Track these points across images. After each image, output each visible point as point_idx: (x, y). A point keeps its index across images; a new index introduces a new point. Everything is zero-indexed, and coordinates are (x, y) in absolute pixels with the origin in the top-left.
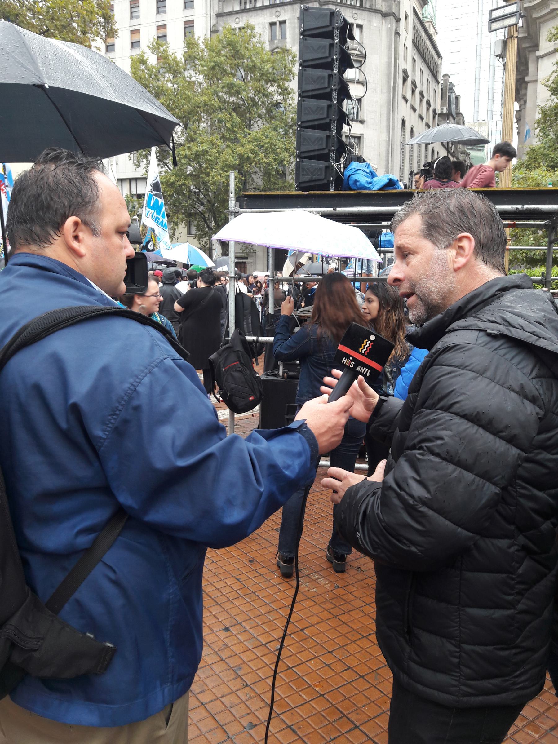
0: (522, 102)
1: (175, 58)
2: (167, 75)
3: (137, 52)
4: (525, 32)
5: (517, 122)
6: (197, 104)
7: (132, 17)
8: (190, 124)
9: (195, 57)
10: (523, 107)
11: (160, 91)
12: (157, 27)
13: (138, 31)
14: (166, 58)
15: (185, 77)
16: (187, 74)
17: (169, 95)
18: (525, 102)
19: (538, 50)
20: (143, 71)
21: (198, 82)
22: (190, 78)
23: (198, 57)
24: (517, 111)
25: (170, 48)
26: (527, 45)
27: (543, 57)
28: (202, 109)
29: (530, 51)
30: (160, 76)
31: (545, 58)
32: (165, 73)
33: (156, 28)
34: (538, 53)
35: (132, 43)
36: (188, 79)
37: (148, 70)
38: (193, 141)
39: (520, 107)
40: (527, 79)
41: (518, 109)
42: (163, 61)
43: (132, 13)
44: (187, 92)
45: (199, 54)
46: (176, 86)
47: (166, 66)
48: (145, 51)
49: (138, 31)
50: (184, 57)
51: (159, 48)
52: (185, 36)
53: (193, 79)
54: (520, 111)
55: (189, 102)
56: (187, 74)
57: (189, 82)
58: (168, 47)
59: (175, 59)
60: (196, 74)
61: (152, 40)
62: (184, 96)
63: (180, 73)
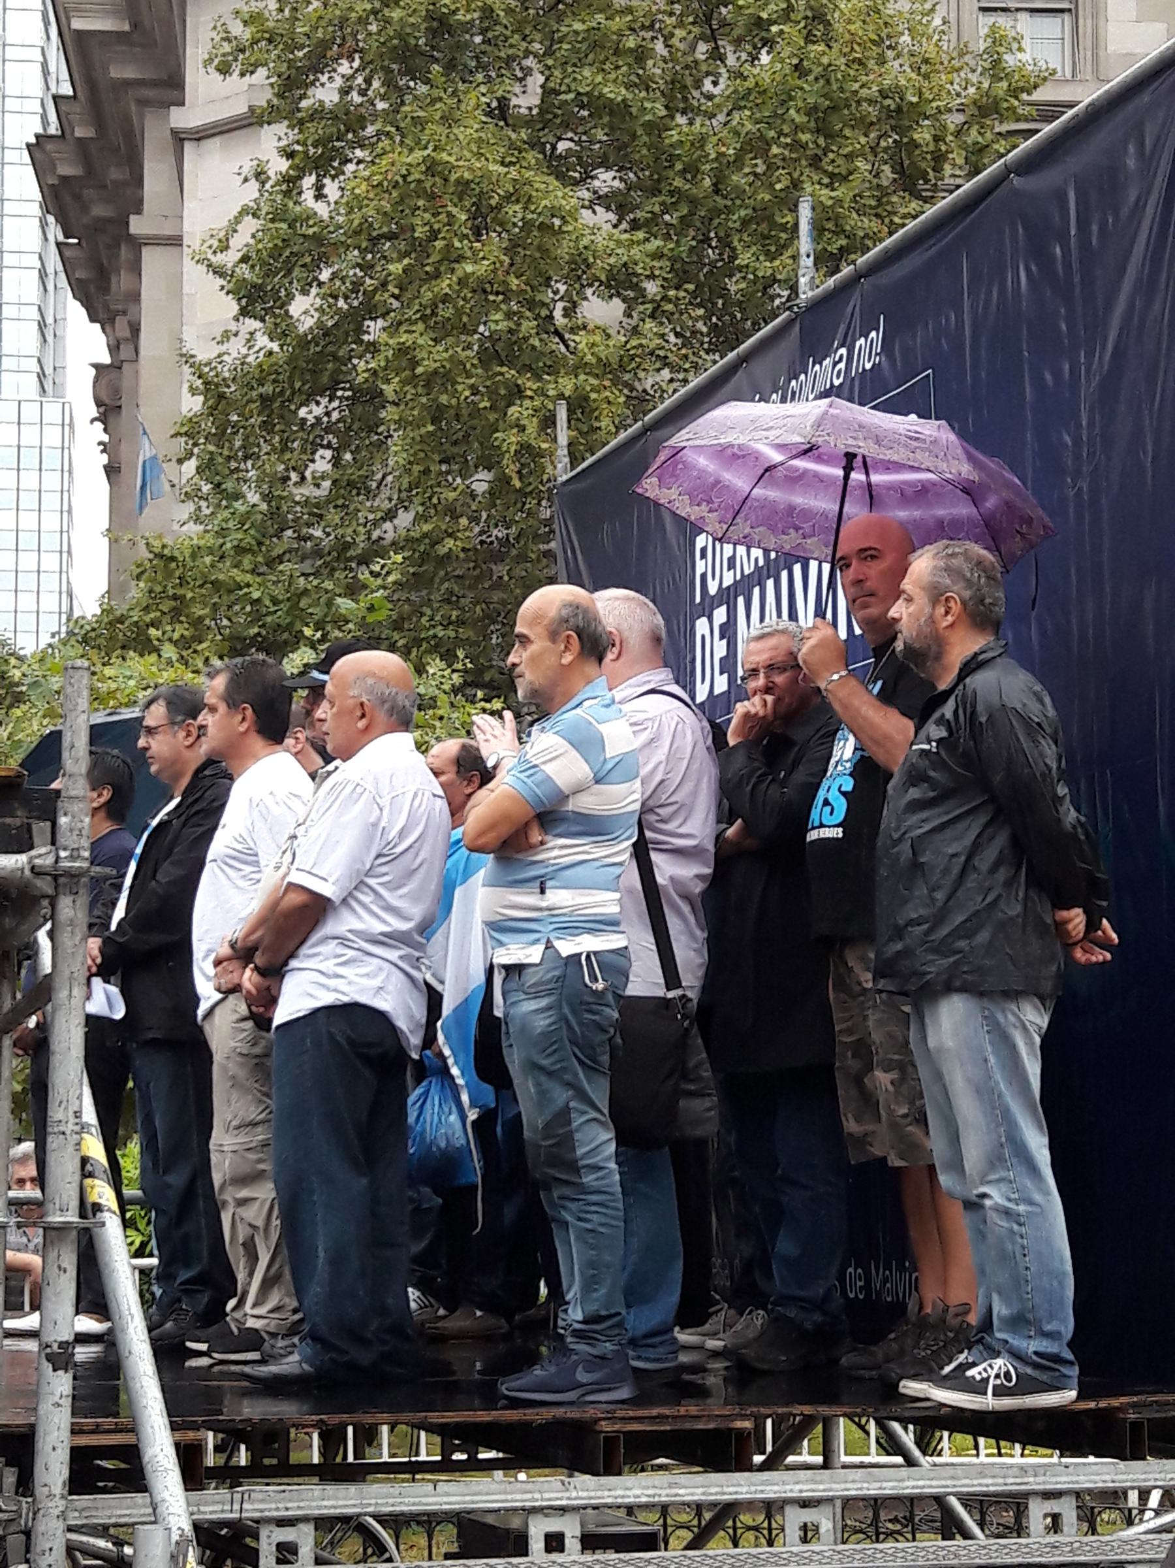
0: (121, 324)
4: (116, 13)
5: (103, 418)
10: (126, 352)
18: (135, 330)
19: (182, 103)
24: (97, 366)
26: (130, 73)
27: (201, 135)
29: (143, 103)
31: (217, 140)
34: (183, 118)
39: (114, 349)
40: (137, 226)
41: (106, 359)
54: (117, 366)
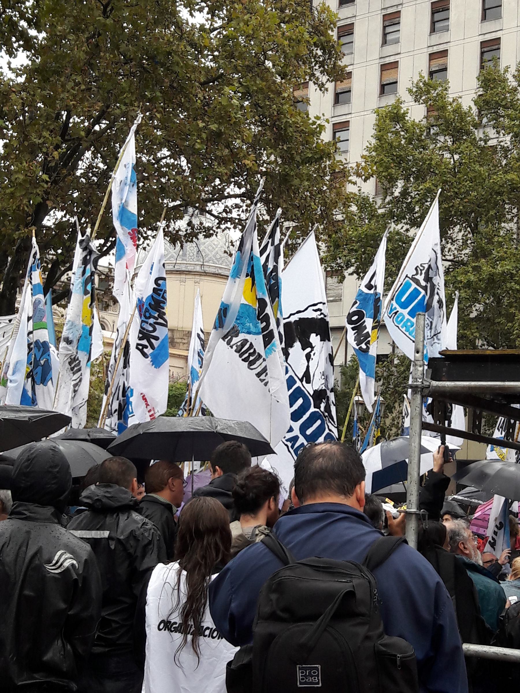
1: (459, 107)
2: (442, 138)
3: (390, 100)
6: (497, 188)
7: (385, 42)
8: (482, 228)
9: (497, 102)
11: (425, 166)
12: (430, 54)
13: (395, 65)
14: (443, 108)
15: (475, 139)
16: (479, 134)
17: (443, 174)
20: (397, 133)
21: (503, 147)
22: (486, 142)
23: (504, 103)
25: (450, 91)
28: (505, 197)
30: (428, 141)
32: (437, 134)
33: (427, 57)
35: (383, 87)
36: (482, 143)
37: (407, 131)
38: (485, 256)
42: (436, 113)
43: (385, 35)
44: (477, 167)
45: (506, 98)
46: (456, 157)
47: (441, 121)
48: (403, 99)
49: (395, 65)
50: (476, 103)
51: (428, 92)
52: (482, 67)
53: (490, 143)
55: (481, 184)
56: (479, 134)
57: (482, 149)
58: (446, 89)
59: (458, 110)
60: (498, 133)
61: (416, 79)
62: (471, 175)
63: (468, 133)
